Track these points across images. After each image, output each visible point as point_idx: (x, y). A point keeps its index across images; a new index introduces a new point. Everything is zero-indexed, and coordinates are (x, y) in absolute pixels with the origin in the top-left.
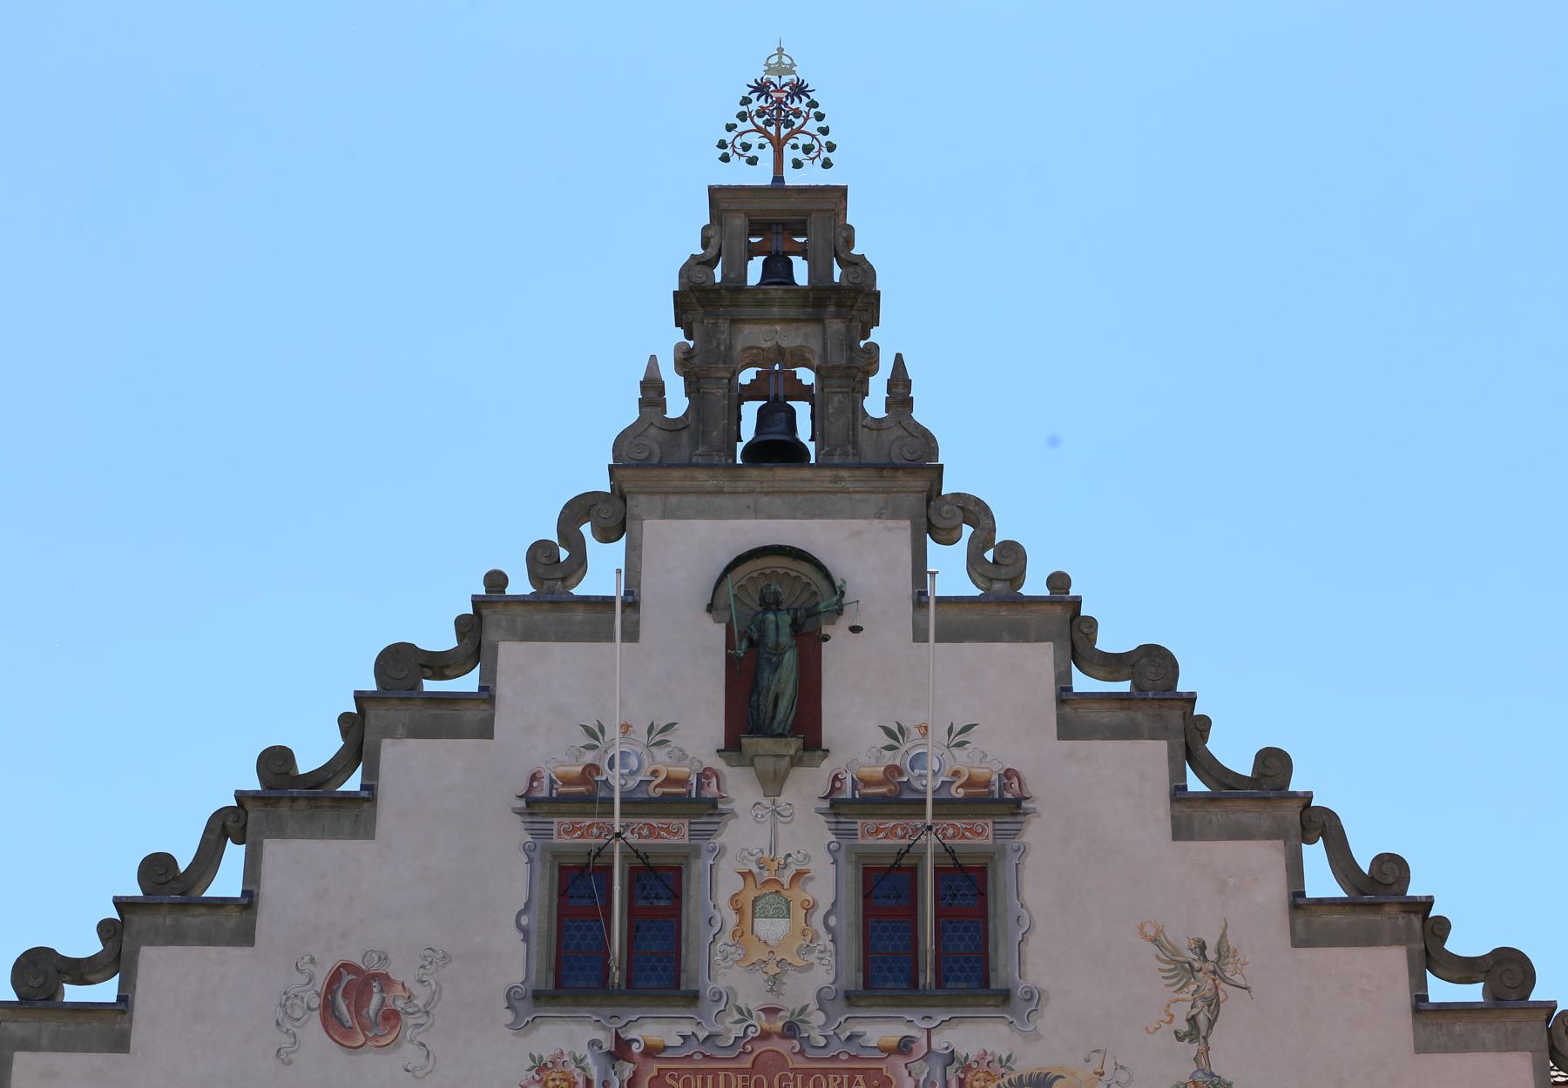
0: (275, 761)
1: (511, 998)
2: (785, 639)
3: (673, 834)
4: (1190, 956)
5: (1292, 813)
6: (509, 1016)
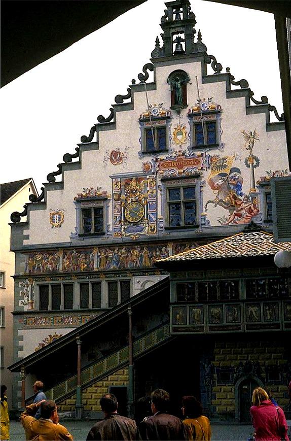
0: (101, 118)
4: (249, 135)
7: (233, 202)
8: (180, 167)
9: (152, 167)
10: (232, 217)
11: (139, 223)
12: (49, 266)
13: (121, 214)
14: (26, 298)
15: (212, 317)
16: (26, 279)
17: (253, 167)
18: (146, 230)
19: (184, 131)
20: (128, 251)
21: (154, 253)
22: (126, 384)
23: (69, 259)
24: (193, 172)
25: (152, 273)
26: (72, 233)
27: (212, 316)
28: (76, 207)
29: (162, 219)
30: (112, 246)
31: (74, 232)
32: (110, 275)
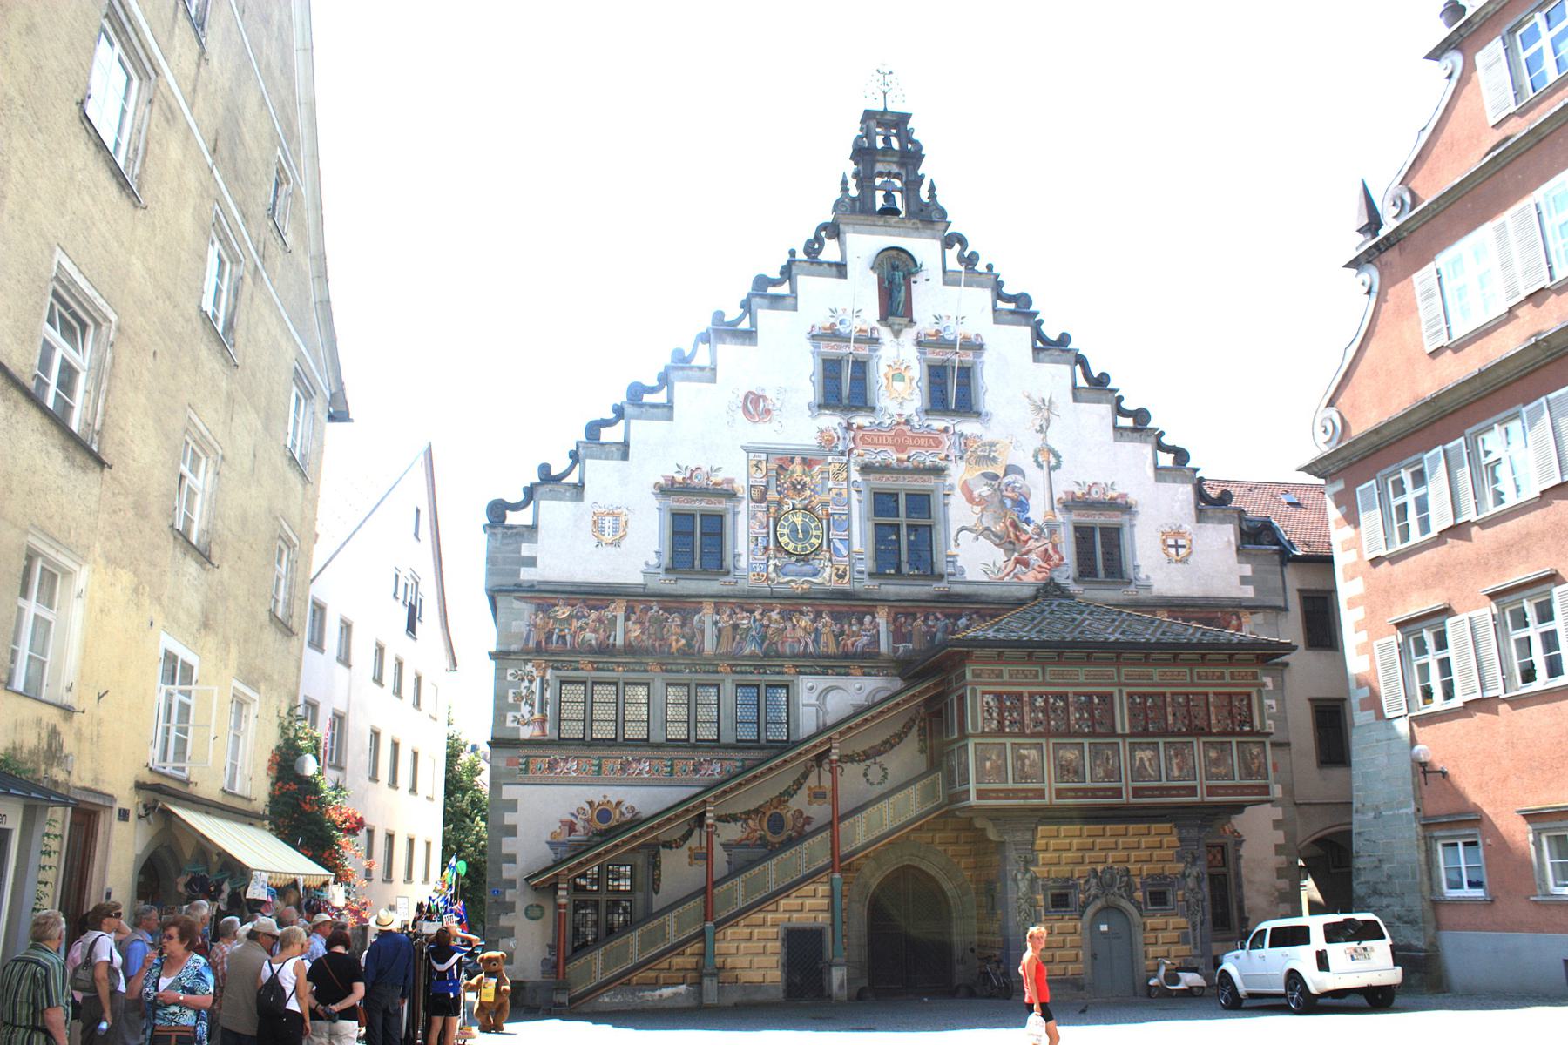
0: (719, 316)
1: (810, 408)
2: (902, 281)
3: (864, 351)
5: (1072, 357)
6: (810, 413)
7: (1012, 535)
8: (901, 448)
9: (839, 438)
10: (1011, 564)
11: (811, 557)
12: (589, 635)
13: (768, 533)
14: (525, 709)
15: (1065, 770)
16: (526, 662)
17: (1051, 469)
18: (826, 575)
19: (907, 375)
20: (786, 616)
21: (846, 627)
22: (823, 919)
23: (640, 622)
24: (928, 463)
25: (843, 671)
26: (647, 564)
27: (1062, 766)
28: (658, 505)
29: (861, 553)
30: (746, 601)
31: (654, 561)
32: (743, 668)
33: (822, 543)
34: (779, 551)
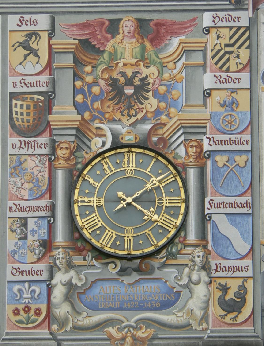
11: (156, 262)
13: (52, 208)
33: (183, 226)
34: (79, 251)
